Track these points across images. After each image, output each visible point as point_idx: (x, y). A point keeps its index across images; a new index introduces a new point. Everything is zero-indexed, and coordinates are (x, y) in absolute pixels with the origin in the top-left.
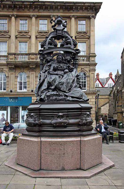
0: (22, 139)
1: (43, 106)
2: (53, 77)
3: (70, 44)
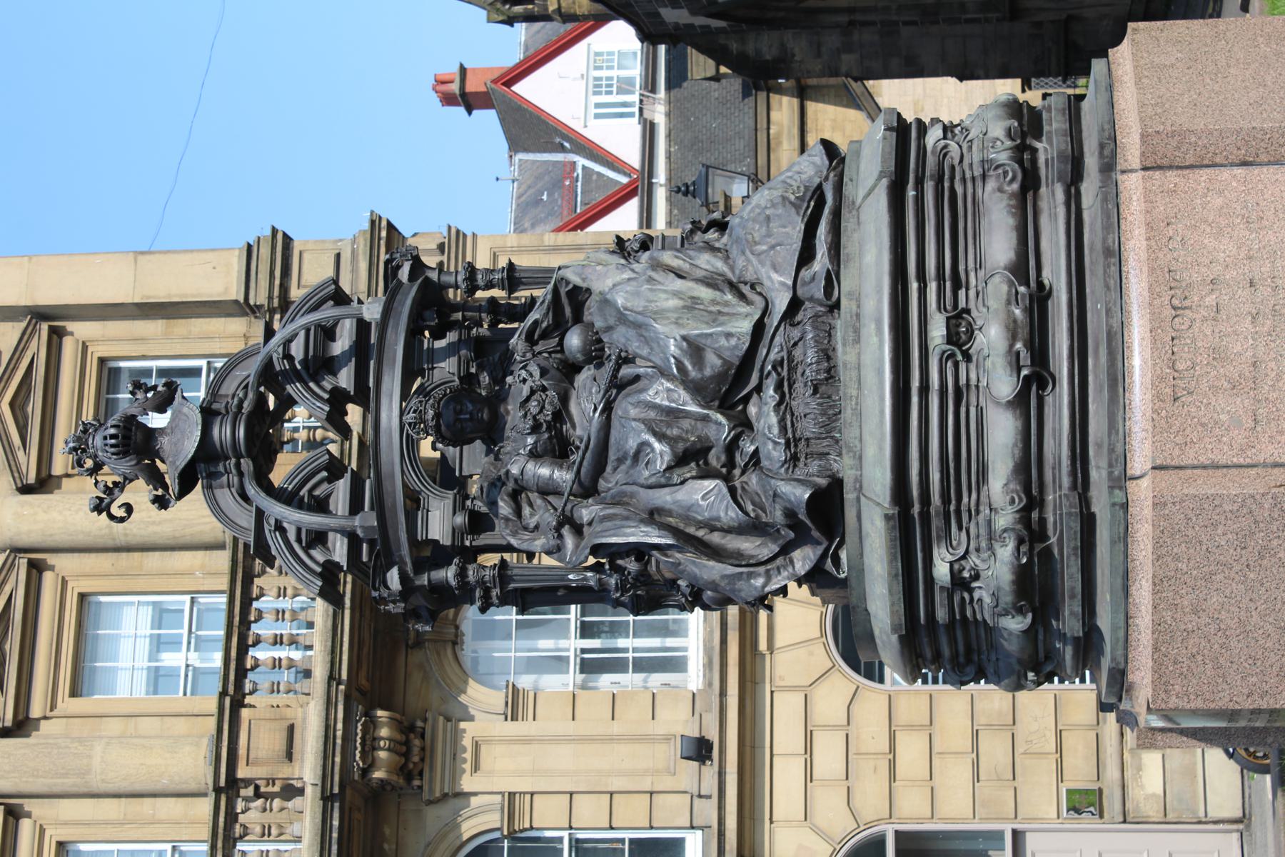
0: (1156, 649)
3: (328, 333)
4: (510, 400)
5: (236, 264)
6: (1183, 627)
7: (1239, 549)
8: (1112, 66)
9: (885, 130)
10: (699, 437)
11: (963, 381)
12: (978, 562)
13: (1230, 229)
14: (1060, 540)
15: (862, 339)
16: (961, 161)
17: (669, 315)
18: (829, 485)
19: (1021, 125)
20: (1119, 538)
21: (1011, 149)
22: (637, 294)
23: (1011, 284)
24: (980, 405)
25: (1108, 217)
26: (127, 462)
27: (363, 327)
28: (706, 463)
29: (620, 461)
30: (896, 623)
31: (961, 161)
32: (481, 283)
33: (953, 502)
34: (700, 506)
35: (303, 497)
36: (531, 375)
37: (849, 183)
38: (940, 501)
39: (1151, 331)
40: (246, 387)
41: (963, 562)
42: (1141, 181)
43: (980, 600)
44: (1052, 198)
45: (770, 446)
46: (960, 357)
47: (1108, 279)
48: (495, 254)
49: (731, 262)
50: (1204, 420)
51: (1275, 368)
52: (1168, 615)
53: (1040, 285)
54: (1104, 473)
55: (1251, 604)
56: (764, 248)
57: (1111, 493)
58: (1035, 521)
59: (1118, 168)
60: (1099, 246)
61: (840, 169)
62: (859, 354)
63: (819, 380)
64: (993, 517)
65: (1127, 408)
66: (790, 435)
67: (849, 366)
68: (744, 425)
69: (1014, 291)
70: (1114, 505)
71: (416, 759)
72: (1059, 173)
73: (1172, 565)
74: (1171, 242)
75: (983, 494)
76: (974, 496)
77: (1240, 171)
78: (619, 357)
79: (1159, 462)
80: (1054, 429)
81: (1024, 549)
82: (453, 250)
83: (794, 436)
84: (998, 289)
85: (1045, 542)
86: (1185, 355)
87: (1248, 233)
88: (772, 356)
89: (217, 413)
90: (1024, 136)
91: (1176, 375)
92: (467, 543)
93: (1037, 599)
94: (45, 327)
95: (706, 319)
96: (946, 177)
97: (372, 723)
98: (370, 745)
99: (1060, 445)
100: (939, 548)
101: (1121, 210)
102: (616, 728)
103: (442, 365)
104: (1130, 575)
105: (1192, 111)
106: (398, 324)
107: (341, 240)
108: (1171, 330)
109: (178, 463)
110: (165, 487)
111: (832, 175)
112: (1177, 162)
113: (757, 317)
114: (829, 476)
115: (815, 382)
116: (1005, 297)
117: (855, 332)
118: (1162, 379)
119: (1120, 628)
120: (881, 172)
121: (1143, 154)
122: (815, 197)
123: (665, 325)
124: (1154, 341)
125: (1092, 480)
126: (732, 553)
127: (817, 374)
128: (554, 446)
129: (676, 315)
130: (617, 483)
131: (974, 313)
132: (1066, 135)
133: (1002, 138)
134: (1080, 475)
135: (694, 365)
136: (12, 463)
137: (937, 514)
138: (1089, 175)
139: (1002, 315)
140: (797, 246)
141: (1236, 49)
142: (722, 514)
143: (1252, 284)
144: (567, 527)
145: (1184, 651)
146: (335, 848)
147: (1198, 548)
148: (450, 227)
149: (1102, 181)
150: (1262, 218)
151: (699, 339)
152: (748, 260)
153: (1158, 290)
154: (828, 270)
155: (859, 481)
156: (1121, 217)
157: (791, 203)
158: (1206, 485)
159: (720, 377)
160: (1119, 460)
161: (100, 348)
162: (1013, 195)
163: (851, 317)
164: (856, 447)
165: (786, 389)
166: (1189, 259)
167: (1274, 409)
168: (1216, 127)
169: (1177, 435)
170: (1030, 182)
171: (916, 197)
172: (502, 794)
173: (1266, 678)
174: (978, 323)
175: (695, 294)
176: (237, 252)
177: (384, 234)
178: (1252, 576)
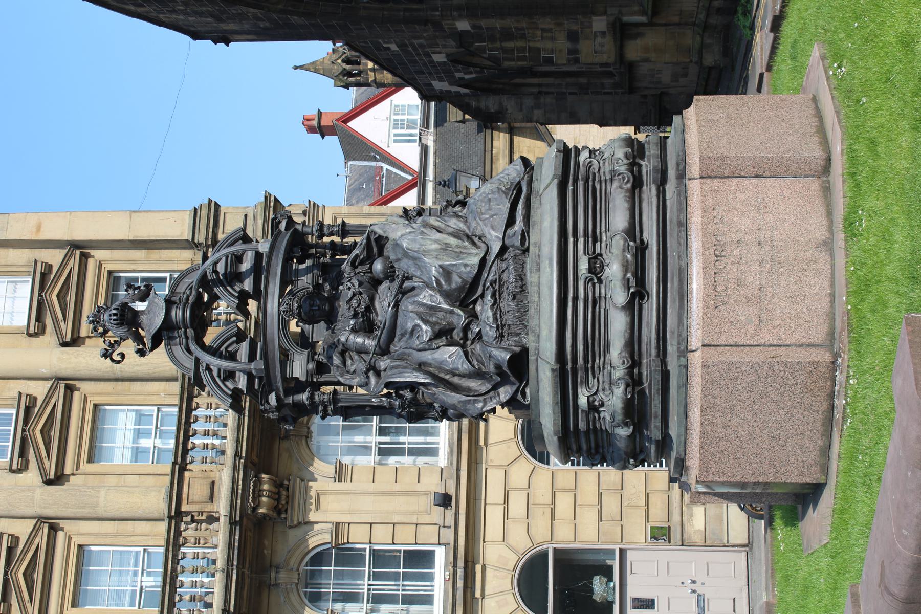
0: (702, 447)
1: (548, 347)
2: (409, 319)
3: (239, 259)
4: (341, 299)
5: (188, 219)
6: (717, 436)
8: (684, 120)
10: (447, 322)
11: (597, 294)
12: (603, 396)
14: (650, 385)
15: (541, 270)
16: (599, 170)
17: (432, 253)
18: (521, 351)
19: (633, 151)
22: (414, 241)
23: (625, 240)
25: (681, 204)
26: (123, 329)
27: (258, 255)
28: (452, 337)
29: (403, 335)
30: (557, 429)
31: (599, 170)
32: (326, 232)
33: (590, 362)
34: (448, 361)
35: (222, 351)
36: (353, 285)
40: (191, 288)
41: (595, 397)
42: (699, 184)
43: (604, 418)
44: (649, 193)
45: (488, 328)
46: (596, 281)
48: (335, 217)
49: (468, 224)
52: (709, 428)
53: (642, 241)
54: (675, 348)
55: (755, 423)
56: (487, 216)
57: (678, 359)
59: (687, 177)
60: (675, 221)
61: (531, 173)
62: (539, 277)
66: (499, 322)
68: (473, 316)
70: (680, 366)
71: (283, 502)
72: (653, 179)
73: (712, 400)
75: (607, 358)
77: (754, 180)
78: (404, 276)
79: (706, 342)
80: (648, 323)
81: (629, 389)
82: (311, 214)
83: (501, 323)
84: (618, 243)
85: (641, 386)
86: (721, 283)
87: (758, 215)
88: (490, 278)
89: (175, 303)
90: (634, 157)
91: (717, 294)
92: (315, 380)
94: (78, 252)
95: (453, 256)
97: (259, 481)
98: (258, 494)
101: (688, 201)
102: (397, 487)
103: (303, 278)
106: (278, 255)
107: (248, 207)
108: (714, 268)
109: (151, 331)
110: (144, 344)
111: (526, 176)
112: (720, 174)
113: (482, 255)
114: (521, 346)
116: (622, 247)
118: (709, 296)
121: (701, 169)
123: (430, 259)
124: (705, 274)
125: (668, 351)
126: (466, 388)
128: (365, 327)
129: (436, 253)
130: (401, 347)
131: (604, 256)
132: (658, 158)
135: (446, 282)
136: (58, 329)
137: (581, 369)
138: (670, 180)
139: (620, 258)
140: (506, 215)
141: (753, 112)
142: (460, 367)
143: (760, 244)
144: (372, 372)
145: (717, 449)
146: (236, 552)
148: (310, 201)
149: (677, 184)
151: (449, 267)
152: (478, 223)
154: (523, 230)
155: (537, 349)
157: (503, 191)
158: (732, 356)
159: (460, 289)
160: (684, 340)
161: (109, 265)
162: (627, 190)
165: (497, 296)
166: (725, 229)
170: (637, 183)
171: (574, 190)
172: (332, 523)
173: (763, 465)
175: (447, 241)
176: (188, 213)
177: (272, 204)
178: (756, 407)
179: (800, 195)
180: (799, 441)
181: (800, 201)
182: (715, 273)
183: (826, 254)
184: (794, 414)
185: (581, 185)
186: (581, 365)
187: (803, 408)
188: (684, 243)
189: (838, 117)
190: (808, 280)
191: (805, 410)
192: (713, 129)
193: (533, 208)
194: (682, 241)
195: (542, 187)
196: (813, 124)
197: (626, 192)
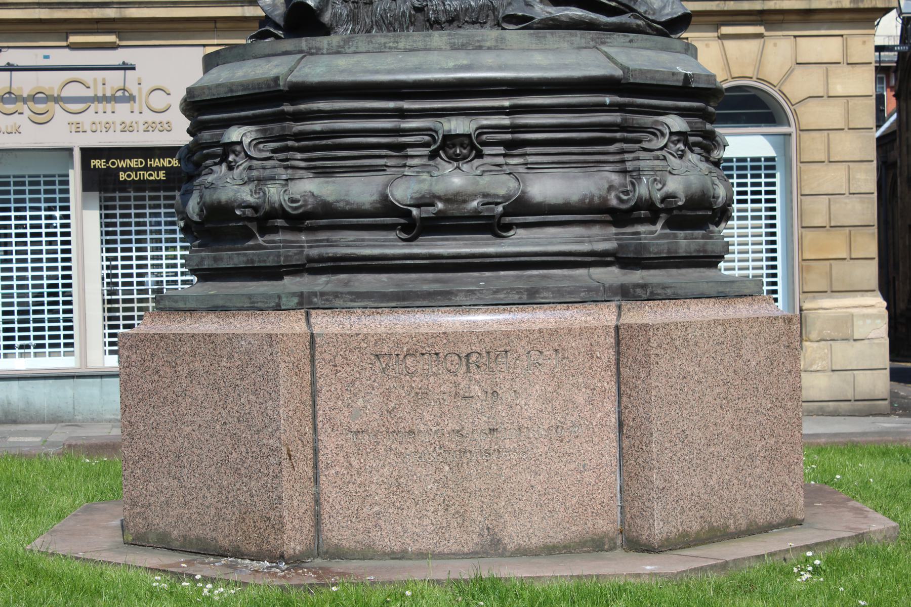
0: (162, 337)
6: (179, 362)
7: (238, 415)
9: (686, 75)
12: (241, 168)
13: (550, 410)
14: (260, 247)
15: (454, 52)
18: (323, 25)
19: (680, 208)
20: (253, 303)
21: (650, 197)
23: (506, 198)
24: (388, 169)
25: (570, 293)
30: (196, 93)
33: (296, 144)
37: (628, 39)
38: (297, 131)
39: (444, 333)
41: (243, 154)
42: (606, 324)
46: (433, 147)
47: (505, 292)
50: (358, 383)
51: (408, 452)
52: (186, 348)
53: (509, 227)
54: (317, 289)
55: (196, 426)
57: (294, 294)
58: (274, 223)
59: (623, 303)
60: (544, 284)
61: (650, 31)
62: (440, 49)
63: (428, 13)
64: (278, 182)
65: (374, 310)
67: (427, 39)
69: (499, 200)
70: (279, 297)
72: (626, 245)
74: (537, 353)
76: (303, 164)
77: (613, 419)
79: (318, 340)
80: (363, 240)
81: (249, 212)
86: (420, 365)
87: (546, 428)
90: (668, 211)
91: (401, 357)
93: (210, 225)
96: (626, 134)
99: (348, 246)
100: (257, 131)
104: (223, 313)
105: (676, 374)
108: (446, 352)
111: (640, 22)
112: (623, 360)
114: (331, 25)
115: (426, 9)
116: (492, 192)
117: (463, 45)
118: (397, 343)
119: (185, 304)
120: (628, 69)
121: (630, 326)
122: (621, 7)
124: (436, 336)
125: (318, 277)
127: (434, 11)
131: (477, 162)
132: (669, 251)
133: (665, 189)
134: (321, 265)
137: (283, 128)
138: (625, 274)
139: (471, 189)
141: (759, 417)
143: (492, 430)
145: (161, 363)
147: (238, 377)
149: (611, 286)
150: (562, 441)
153: (487, 340)
154: (533, 18)
155: (318, 52)
156: (570, 305)
162: (605, 200)
163: (478, 41)
164: (349, 48)
166: (518, 371)
167: (368, 450)
168: (653, 398)
169: (343, 358)
171: (604, 105)
173: (143, 439)
174: (465, 166)
178: (218, 427)
179: (586, 500)
180: (176, 498)
181: (574, 500)
182: (437, 354)
183: (477, 544)
184: (211, 490)
185: (615, 118)
186: (293, 127)
187: (220, 505)
188: (497, 299)
189: (712, 567)
190: (429, 514)
191: (217, 508)
192: (718, 348)
193: (572, 35)
194: (502, 296)
195: (611, 51)
196: (731, 521)
197: (600, 197)
